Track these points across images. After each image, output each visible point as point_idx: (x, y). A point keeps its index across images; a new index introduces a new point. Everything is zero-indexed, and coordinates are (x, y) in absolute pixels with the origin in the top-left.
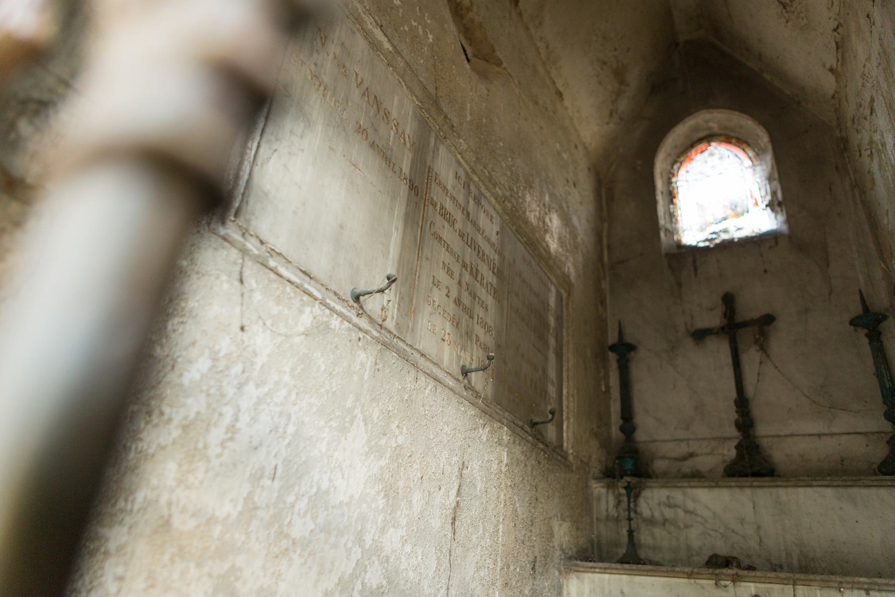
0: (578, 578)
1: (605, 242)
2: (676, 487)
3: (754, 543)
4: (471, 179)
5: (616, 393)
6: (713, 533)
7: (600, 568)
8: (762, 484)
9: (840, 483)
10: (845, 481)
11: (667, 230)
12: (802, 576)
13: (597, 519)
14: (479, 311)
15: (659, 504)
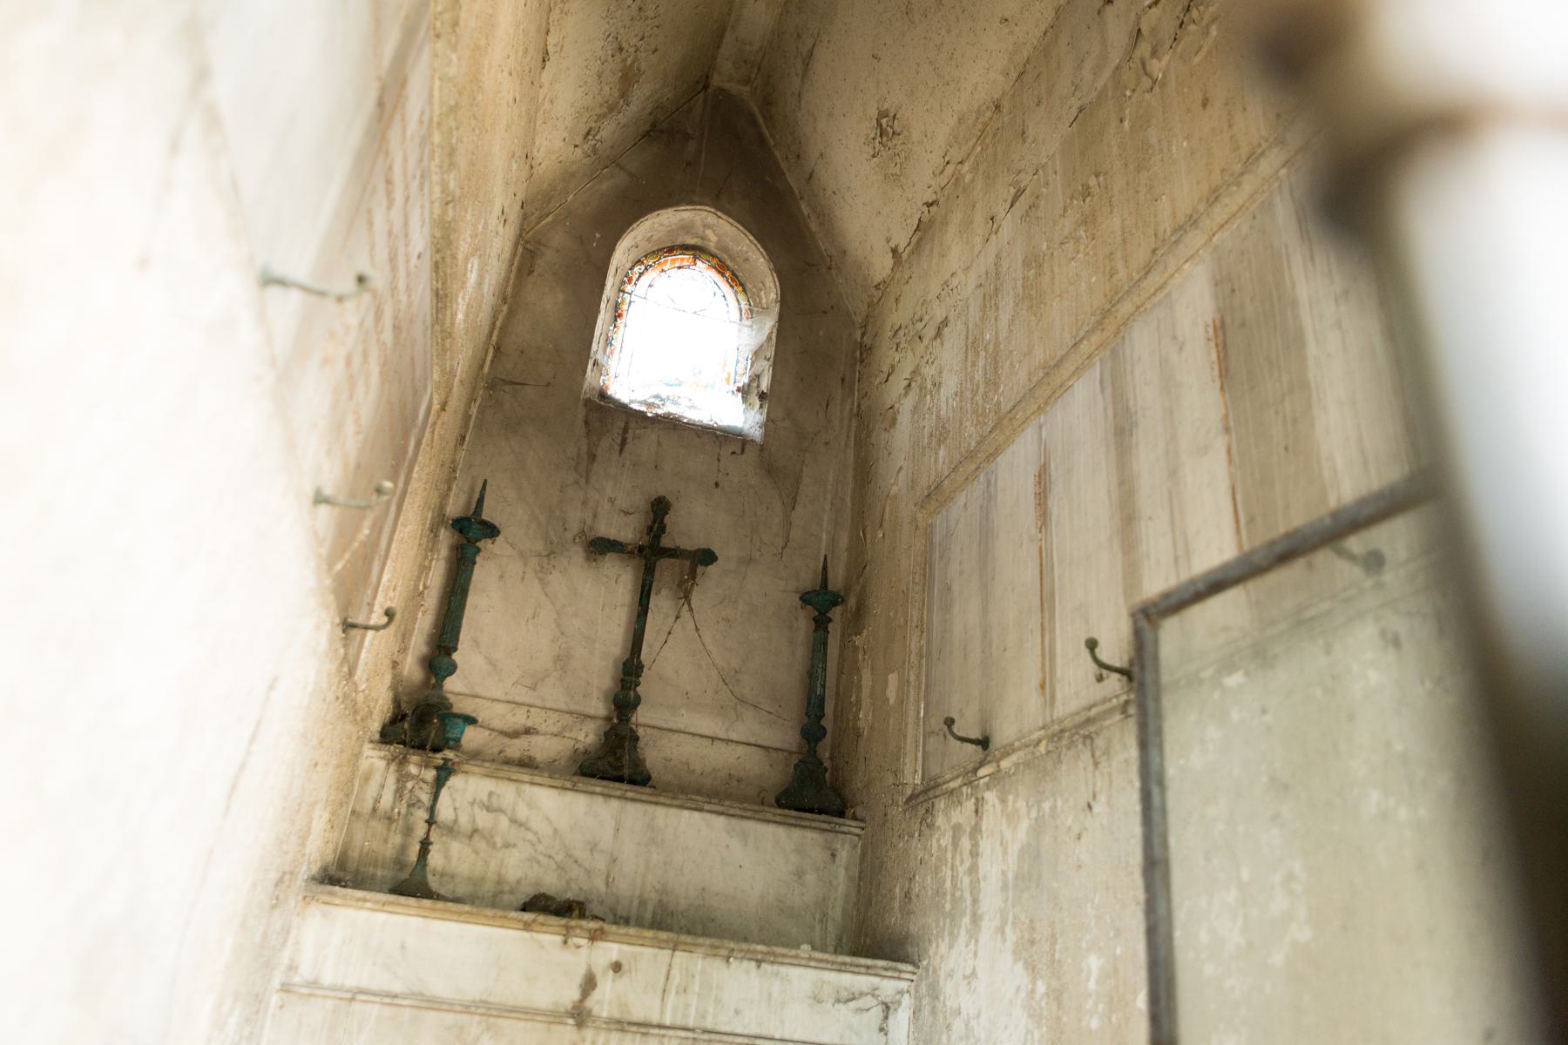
0: (324, 915)
1: (494, 338)
2: (510, 779)
3: (599, 884)
4: (430, 134)
5: (431, 601)
6: (543, 860)
7: (377, 902)
8: (639, 797)
9: (739, 812)
10: (745, 809)
11: (596, 363)
12: (689, 939)
13: (353, 812)
14: (360, 390)
15: (472, 804)
